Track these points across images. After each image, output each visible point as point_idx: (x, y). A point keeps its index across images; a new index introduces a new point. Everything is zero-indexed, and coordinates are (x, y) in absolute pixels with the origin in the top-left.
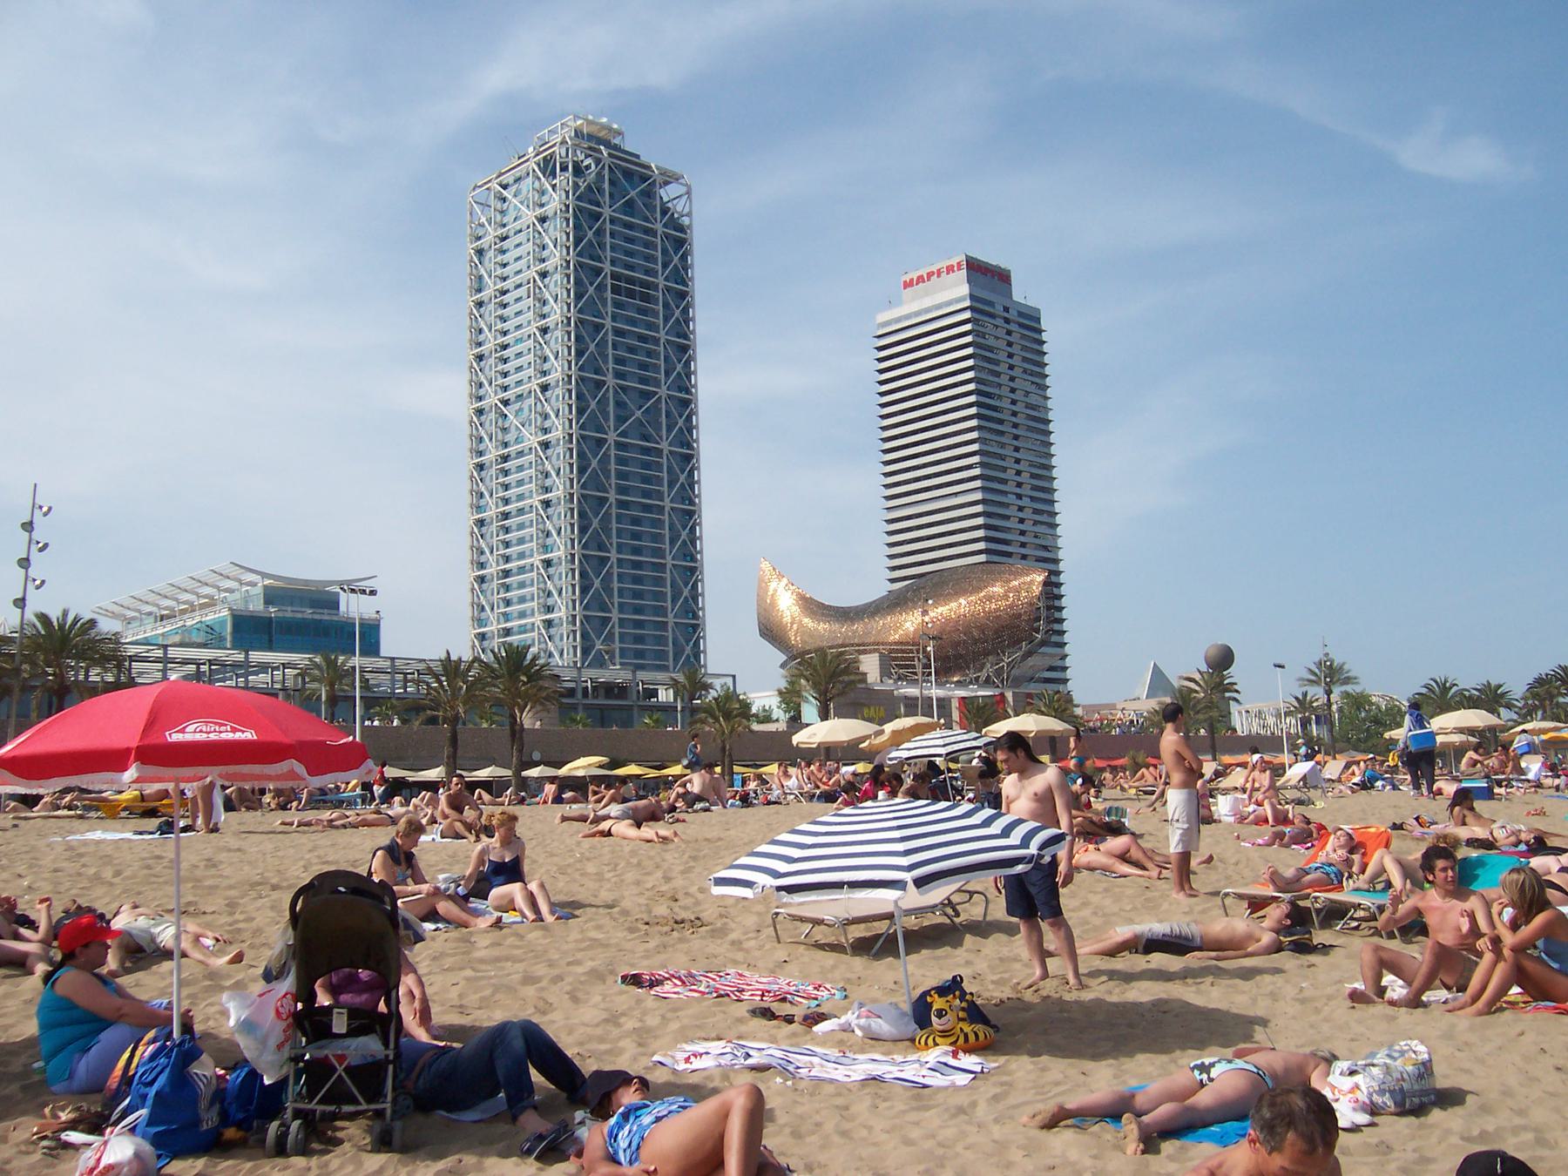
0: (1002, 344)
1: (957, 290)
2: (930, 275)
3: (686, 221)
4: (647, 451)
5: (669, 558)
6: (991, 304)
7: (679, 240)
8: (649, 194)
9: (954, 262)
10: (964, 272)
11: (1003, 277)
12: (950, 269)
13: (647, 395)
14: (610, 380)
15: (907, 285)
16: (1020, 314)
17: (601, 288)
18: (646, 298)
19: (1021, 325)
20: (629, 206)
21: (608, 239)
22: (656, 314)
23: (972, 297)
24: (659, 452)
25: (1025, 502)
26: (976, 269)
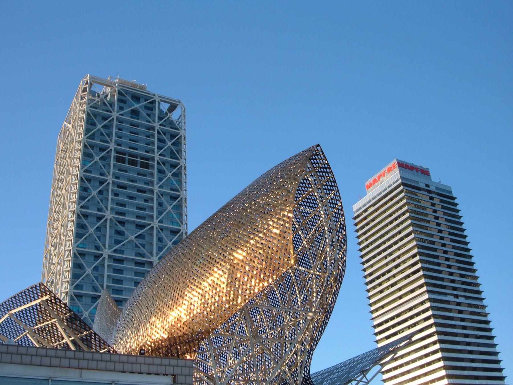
0: (428, 205)
6: (418, 182)
9: (390, 165)
11: (425, 172)
12: (390, 170)
16: (437, 188)
18: (147, 166)
20: (135, 113)
21: (114, 130)
25: (461, 300)
26: (402, 165)
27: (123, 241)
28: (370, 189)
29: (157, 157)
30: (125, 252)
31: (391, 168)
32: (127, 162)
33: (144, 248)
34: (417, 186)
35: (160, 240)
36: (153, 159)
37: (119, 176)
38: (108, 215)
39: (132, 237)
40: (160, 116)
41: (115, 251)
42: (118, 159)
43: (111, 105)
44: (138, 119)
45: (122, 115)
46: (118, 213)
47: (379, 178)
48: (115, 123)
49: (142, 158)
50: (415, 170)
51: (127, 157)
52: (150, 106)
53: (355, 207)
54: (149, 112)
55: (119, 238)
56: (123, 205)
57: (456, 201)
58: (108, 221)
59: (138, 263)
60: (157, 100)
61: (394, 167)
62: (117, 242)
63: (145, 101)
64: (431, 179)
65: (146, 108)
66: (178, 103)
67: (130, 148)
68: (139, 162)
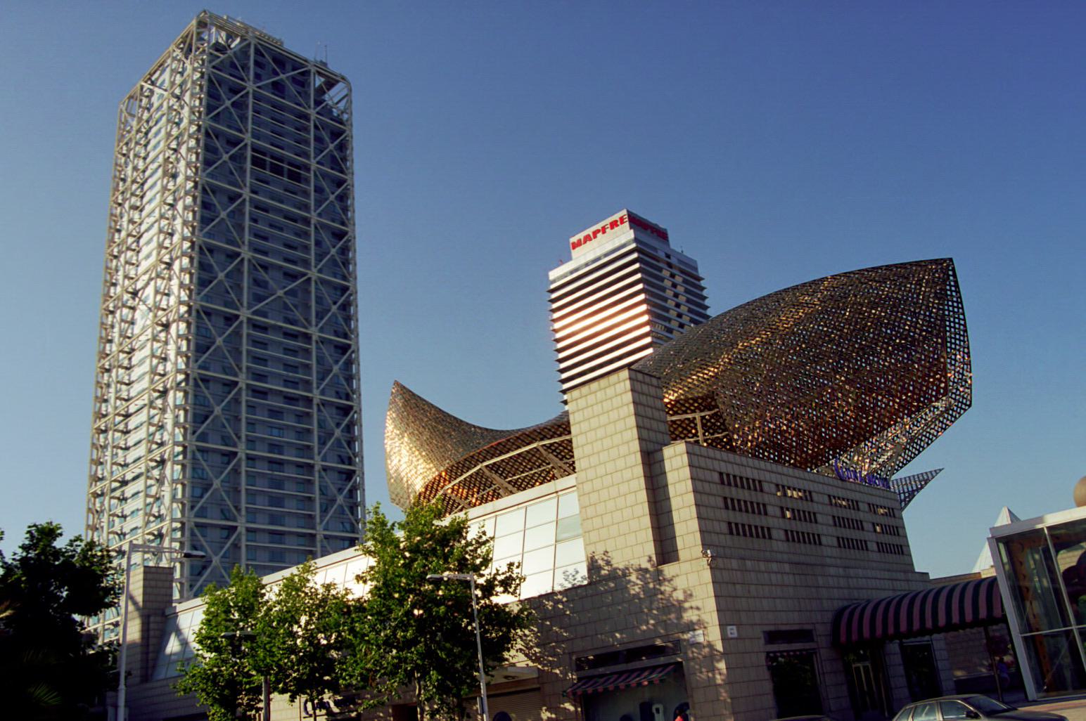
1: (625, 235)
2: (595, 233)
3: (345, 117)
4: (294, 336)
5: (317, 458)
6: (655, 249)
7: (336, 135)
8: (302, 81)
9: (616, 217)
10: (627, 225)
11: (662, 235)
12: (614, 225)
13: (293, 276)
14: (246, 253)
15: (575, 246)
16: (680, 261)
17: (238, 158)
18: (295, 177)
19: (683, 272)
20: (278, 88)
22: (306, 194)
23: (636, 240)
24: (307, 338)
26: (636, 222)
27: (267, 298)
28: (577, 249)
29: (314, 165)
30: (270, 315)
31: (616, 221)
32: (268, 167)
33: (297, 309)
34: (655, 253)
35: (319, 300)
36: (308, 169)
37: (257, 190)
38: (246, 253)
39: (280, 293)
40: (319, 99)
41: (255, 313)
42: (256, 161)
43: (245, 67)
44: (283, 98)
45: (259, 87)
46: (257, 250)
47: (595, 233)
48: (251, 100)
49: (290, 164)
50: (649, 231)
51: (268, 159)
52: (300, 78)
53: (553, 274)
54: (300, 89)
55: (260, 291)
56: (265, 239)
57: (703, 283)
58: (246, 263)
59: (288, 335)
60: (313, 70)
61: (622, 222)
62: (259, 299)
63: (294, 69)
64: (669, 245)
65: (294, 80)
66: (338, 79)
67: (272, 144)
68: (286, 170)
